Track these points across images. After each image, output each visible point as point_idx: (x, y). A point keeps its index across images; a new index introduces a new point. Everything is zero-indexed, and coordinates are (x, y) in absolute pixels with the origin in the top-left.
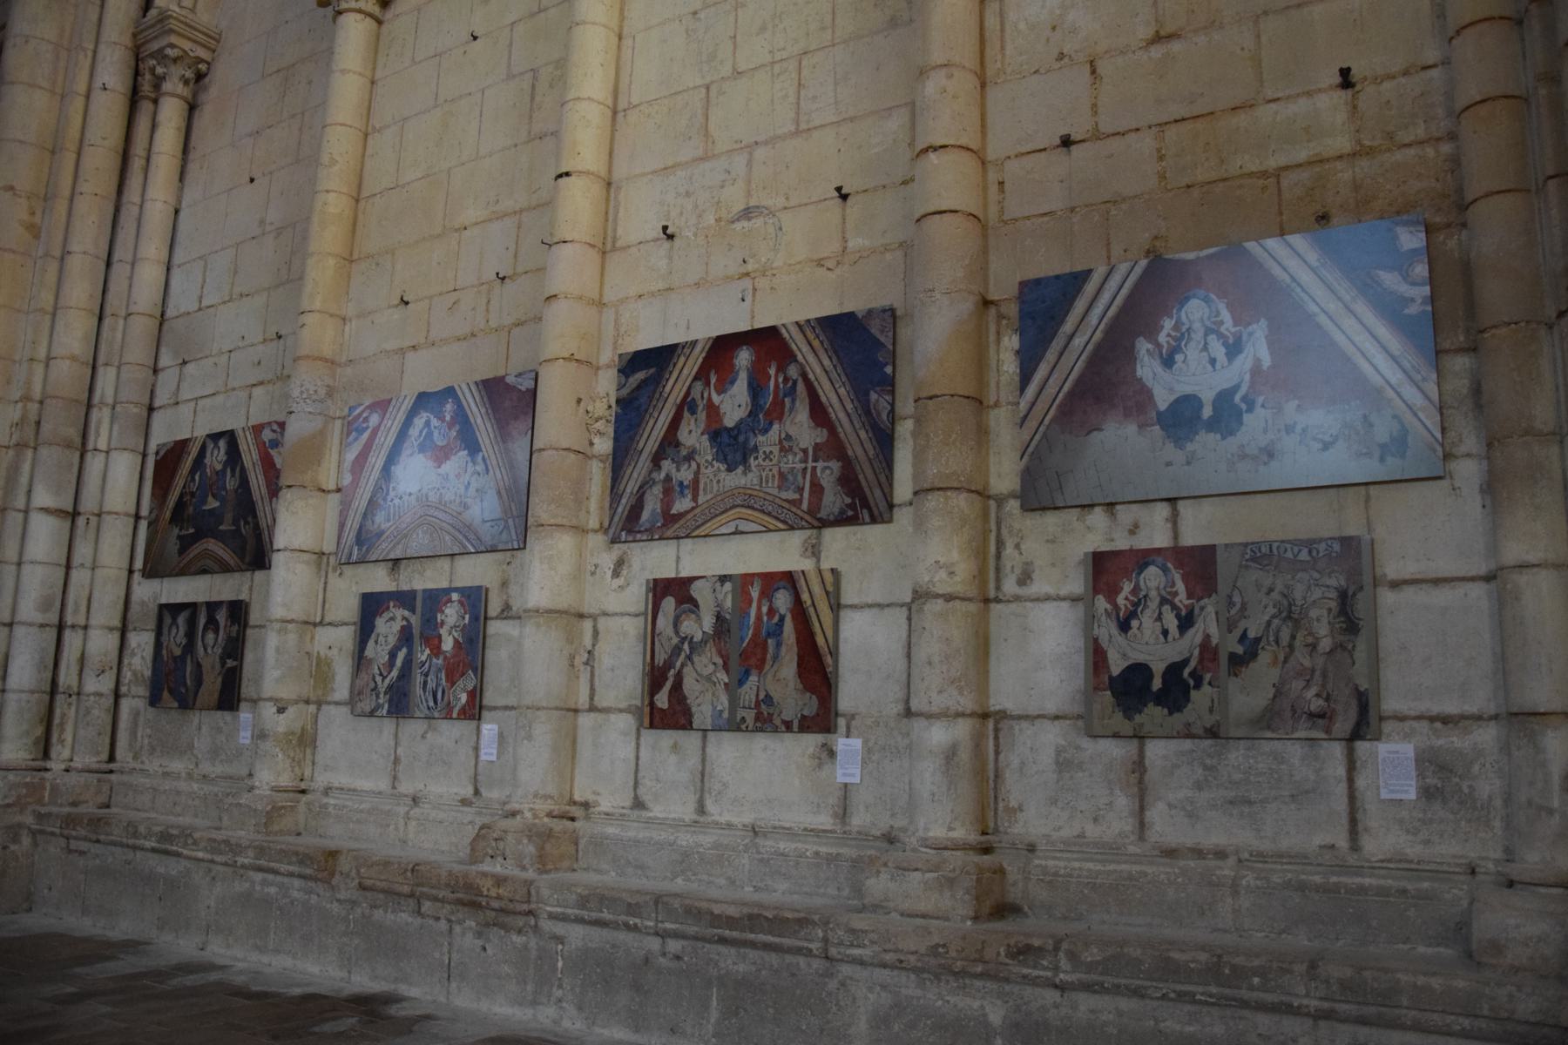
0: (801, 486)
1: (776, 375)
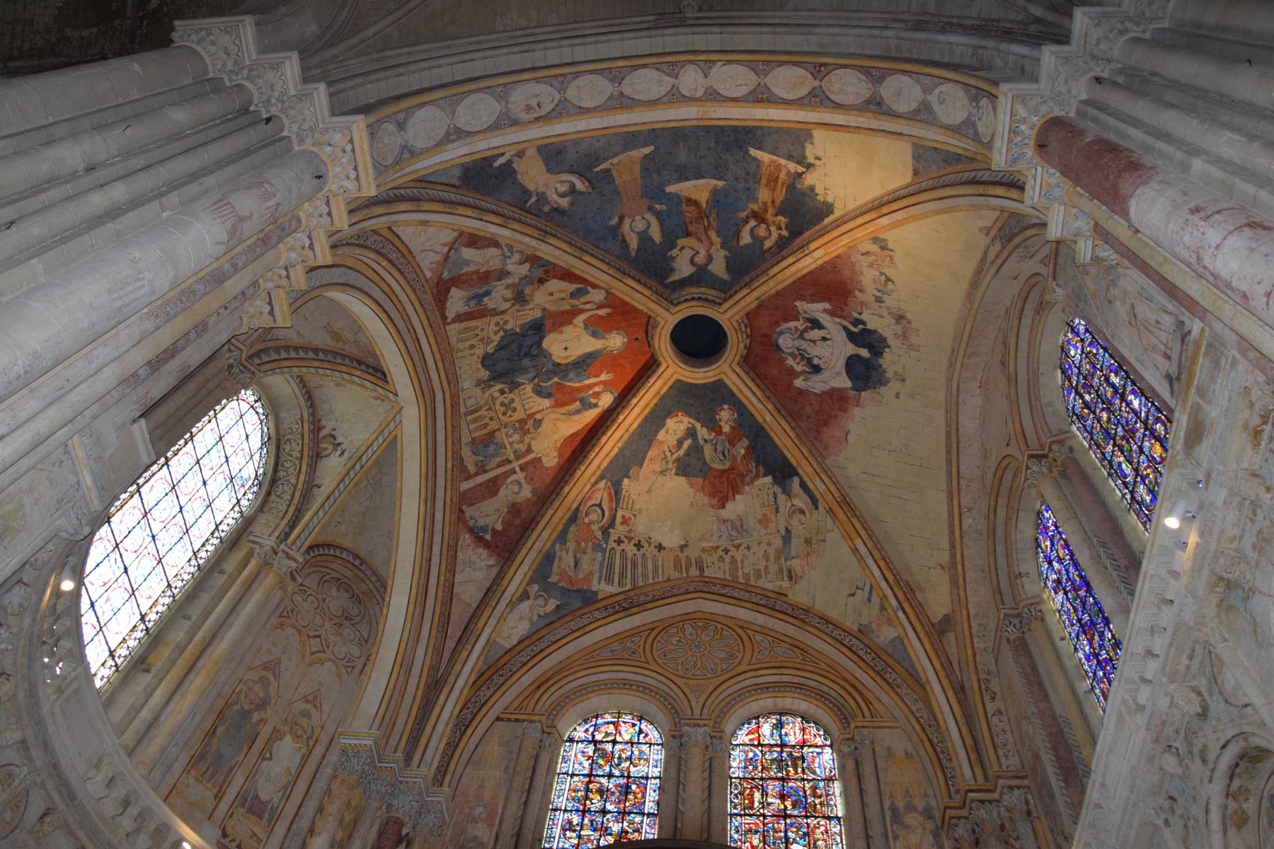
0: (487, 468)
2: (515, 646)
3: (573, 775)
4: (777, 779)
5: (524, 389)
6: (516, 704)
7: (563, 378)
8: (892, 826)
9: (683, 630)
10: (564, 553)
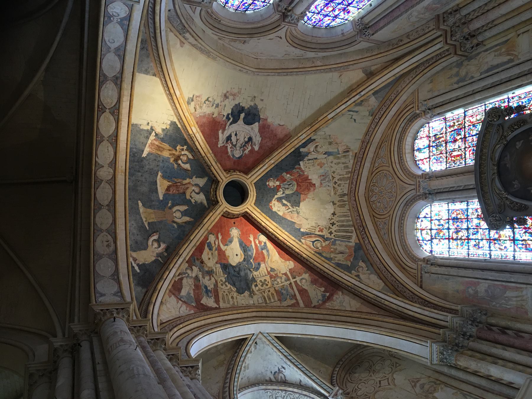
0: (293, 294)
1: (254, 240)
2: (383, 281)
3: (449, 248)
4: (446, 146)
5: (255, 275)
6: (414, 279)
7: (251, 257)
8: (467, 81)
9: (373, 201)
10: (336, 259)
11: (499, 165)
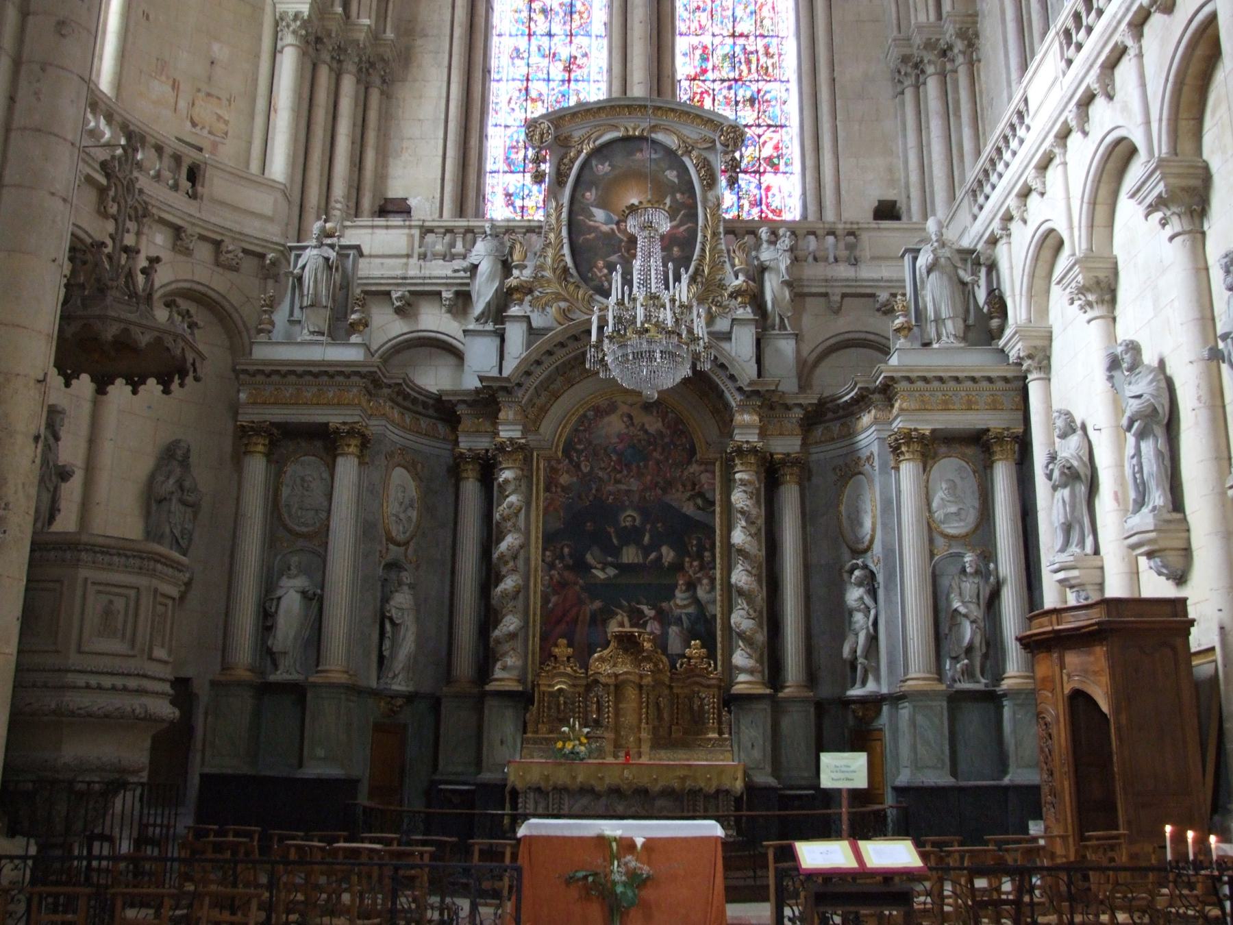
11: (642, 138)
